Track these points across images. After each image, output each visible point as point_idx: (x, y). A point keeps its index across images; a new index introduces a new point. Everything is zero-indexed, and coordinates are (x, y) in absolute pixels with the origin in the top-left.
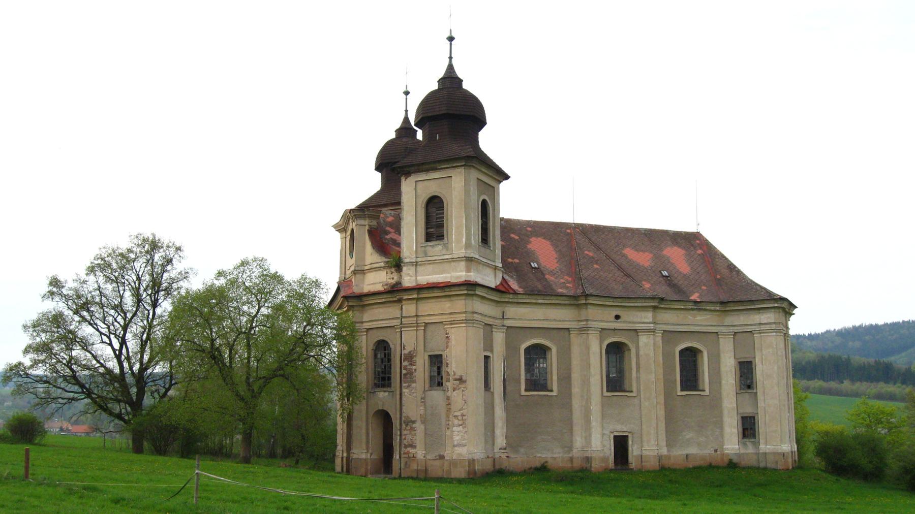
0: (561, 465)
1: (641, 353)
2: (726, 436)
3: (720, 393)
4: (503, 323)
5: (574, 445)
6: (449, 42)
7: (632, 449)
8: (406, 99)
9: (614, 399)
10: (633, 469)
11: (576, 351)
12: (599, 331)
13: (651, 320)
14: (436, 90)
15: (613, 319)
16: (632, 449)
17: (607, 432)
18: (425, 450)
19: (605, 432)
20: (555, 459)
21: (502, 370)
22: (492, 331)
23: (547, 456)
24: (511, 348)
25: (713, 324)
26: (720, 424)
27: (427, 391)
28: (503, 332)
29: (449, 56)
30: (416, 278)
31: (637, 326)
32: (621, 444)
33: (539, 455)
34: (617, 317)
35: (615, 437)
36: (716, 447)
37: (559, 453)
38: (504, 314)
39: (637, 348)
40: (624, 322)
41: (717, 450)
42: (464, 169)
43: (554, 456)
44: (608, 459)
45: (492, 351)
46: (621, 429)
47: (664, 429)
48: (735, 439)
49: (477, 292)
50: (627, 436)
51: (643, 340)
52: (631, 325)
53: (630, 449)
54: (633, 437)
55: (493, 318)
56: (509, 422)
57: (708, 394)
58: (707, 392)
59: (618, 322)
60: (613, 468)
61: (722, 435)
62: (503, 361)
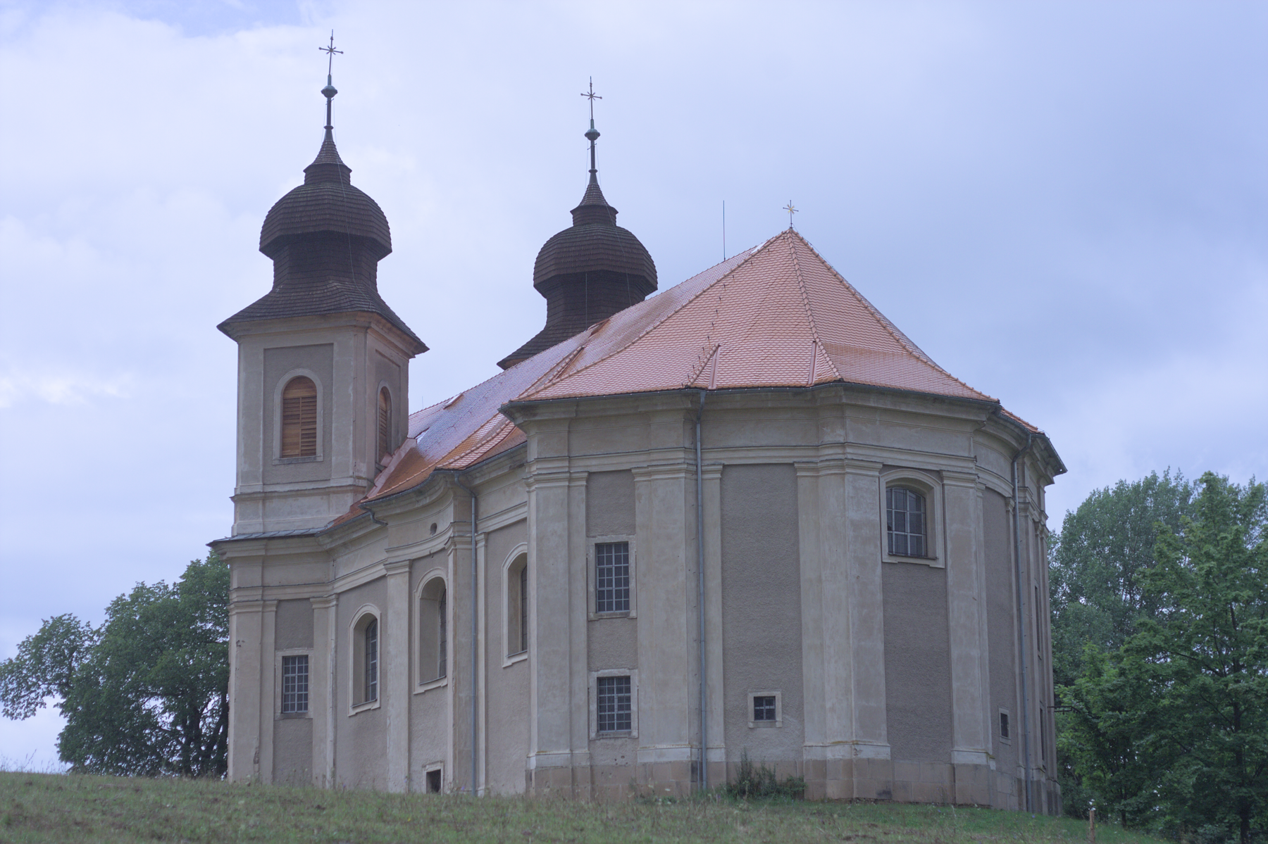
6: (326, 99)
9: (429, 695)
15: (428, 535)
45: (311, 646)
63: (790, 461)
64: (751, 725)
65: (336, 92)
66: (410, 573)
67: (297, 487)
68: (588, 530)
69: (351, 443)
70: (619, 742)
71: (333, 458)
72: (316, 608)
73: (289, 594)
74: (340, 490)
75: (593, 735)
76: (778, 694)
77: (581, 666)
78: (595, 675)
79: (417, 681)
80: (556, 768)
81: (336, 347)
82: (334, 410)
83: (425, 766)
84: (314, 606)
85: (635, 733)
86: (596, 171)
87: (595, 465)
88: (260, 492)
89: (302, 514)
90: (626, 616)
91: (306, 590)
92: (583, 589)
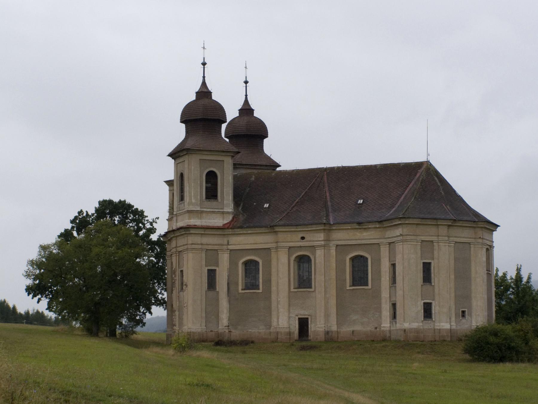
0: (264, 337)
1: (317, 261)
2: (383, 318)
3: (380, 287)
4: (228, 247)
5: (272, 324)
6: (203, 66)
7: (311, 327)
8: (246, 87)
10: (311, 340)
11: (274, 262)
12: (287, 248)
13: (323, 239)
14: (194, 101)
16: (311, 327)
17: (293, 316)
18: (179, 327)
19: (291, 315)
20: (260, 333)
21: (227, 277)
22: (218, 254)
23: (255, 331)
24: (233, 263)
25: (377, 237)
26: (379, 309)
27: (180, 292)
28: (228, 253)
29: (203, 76)
30: (176, 224)
31: (315, 243)
32: (303, 324)
33: (250, 330)
34: (303, 238)
35: (299, 319)
36: (376, 326)
37: (263, 329)
38: (229, 242)
39: (315, 258)
40: (307, 241)
41: (377, 327)
42: (188, 156)
43: (260, 331)
44: (294, 333)
45: (218, 266)
46: (304, 313)
47: (336, 313)
48: (388, 320)
49: (191, 232)
50: (308, 318)
51: (319, 253)
52: (311, 243)
53: (309, 326)
54: (311, 319)
55: (219, 245)
56: (230, 310)
57: (371, 288)
58: (370, 287)
59: (303, 242)
60: (298, 339)
61: (380, 317)
62: (227, 271)
63: (469, 242)
64: (461, 319)
65: (206, 64)
66: (288, 251)
67: (212, 210)
68: (421, 258)
69: (231, 197)
70: (429, 322)
71: (225, 202)
72: (219, 253)
73: (210, 247)
74: (228, 213)
75: (423, 319)
76: (466, 310)
77: (420, 299)
78: (423, 302)
79: (292, 287)
80: (414, 329)
81: (225, 161)
82: (225, 184)
83: (298, 315)
84: (219, 253)
85: (434, 320)
86: (247, 95)
87: (423, 238)
88: (199, 211)
89: (214, 219)
90: (431, 285)
91: (216, 246)
92: (420, 275)
